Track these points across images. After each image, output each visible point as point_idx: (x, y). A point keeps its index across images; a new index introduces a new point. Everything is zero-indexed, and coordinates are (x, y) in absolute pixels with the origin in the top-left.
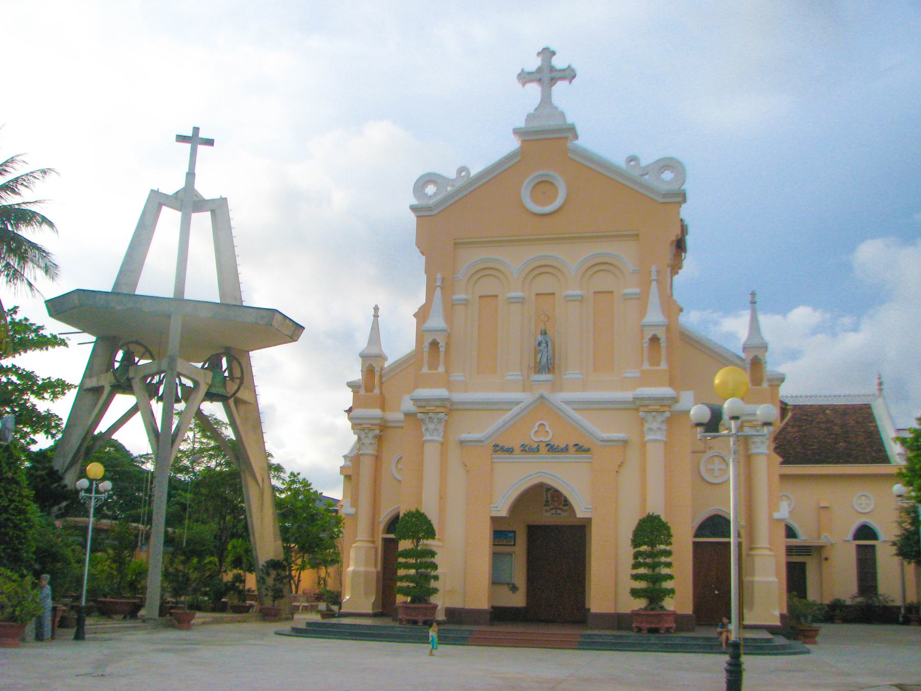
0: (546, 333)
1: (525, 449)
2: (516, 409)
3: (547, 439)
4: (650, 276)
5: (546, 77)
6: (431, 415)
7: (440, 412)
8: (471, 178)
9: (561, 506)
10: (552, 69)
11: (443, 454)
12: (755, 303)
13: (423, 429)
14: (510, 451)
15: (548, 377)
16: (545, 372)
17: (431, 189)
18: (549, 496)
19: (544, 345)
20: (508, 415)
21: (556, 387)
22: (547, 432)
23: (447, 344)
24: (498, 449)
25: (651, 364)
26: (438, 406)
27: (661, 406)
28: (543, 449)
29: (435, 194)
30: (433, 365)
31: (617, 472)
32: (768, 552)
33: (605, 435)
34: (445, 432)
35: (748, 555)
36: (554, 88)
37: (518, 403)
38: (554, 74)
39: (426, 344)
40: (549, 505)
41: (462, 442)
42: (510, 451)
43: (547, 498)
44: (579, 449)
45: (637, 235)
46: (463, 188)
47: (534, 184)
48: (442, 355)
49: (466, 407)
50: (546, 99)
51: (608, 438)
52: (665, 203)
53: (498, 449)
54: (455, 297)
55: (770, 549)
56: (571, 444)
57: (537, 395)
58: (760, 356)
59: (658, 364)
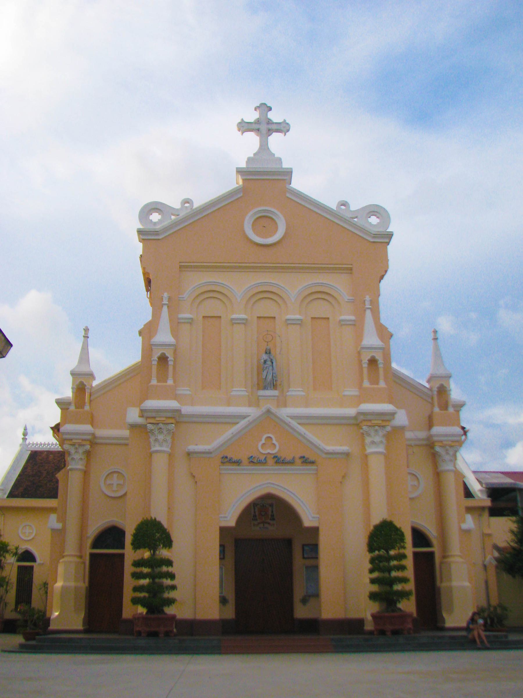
0: (270, 353)
1: (252, 461)
2: (243, 423)
3: (274, 452)
4: (365, 305)
5: (264, 127)
6: (161, 425)
7: (169, 423)
8: (193, 210)
9: (269, 521)
10: (269, 122)
11: (171, 465)
12: (437, 339)
13: (152, 440)
14: (238, 463)
15: (276, 393)
16: (271, 388)
17: (155, 217)
18: (256, 510)
19: (269, 363)
20: (235, 429)
21: (283, 402)
22: (274, 444)
23: (175, 358)
24: (226, 460)
25: (371, 383)
26: (167, 418)
27: (383, 421)
28: (271, 461)
29: (160, 221)
30: (162, 377)
31: (341, 482)
32: (460, 560)
33: (330, 448)
34: (173, 443)
35: (441, 563)
36: (270, 138)
37: (244, 417)
38: (270, 127)
39: (155, 357)
40: (257, 520)
41: (189, 454)
42: (238, 463)
43: (255, 512)
44: (305, 461)
45: (351, 269)
46: (184, 220)
47: (255, 218)
48: (171, 368)
49: (195, 419)
50: (264, 147)
51: (333, 450)
52: (374, 242)
53: (226, 460)
54: (180, 316)
55: (461, 557)
56: (298, 456)
57: (263, 409)
58: (445, 385)
59: (377, 383)
